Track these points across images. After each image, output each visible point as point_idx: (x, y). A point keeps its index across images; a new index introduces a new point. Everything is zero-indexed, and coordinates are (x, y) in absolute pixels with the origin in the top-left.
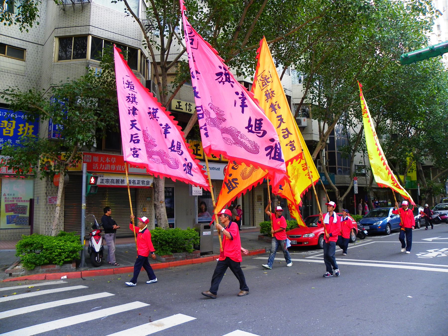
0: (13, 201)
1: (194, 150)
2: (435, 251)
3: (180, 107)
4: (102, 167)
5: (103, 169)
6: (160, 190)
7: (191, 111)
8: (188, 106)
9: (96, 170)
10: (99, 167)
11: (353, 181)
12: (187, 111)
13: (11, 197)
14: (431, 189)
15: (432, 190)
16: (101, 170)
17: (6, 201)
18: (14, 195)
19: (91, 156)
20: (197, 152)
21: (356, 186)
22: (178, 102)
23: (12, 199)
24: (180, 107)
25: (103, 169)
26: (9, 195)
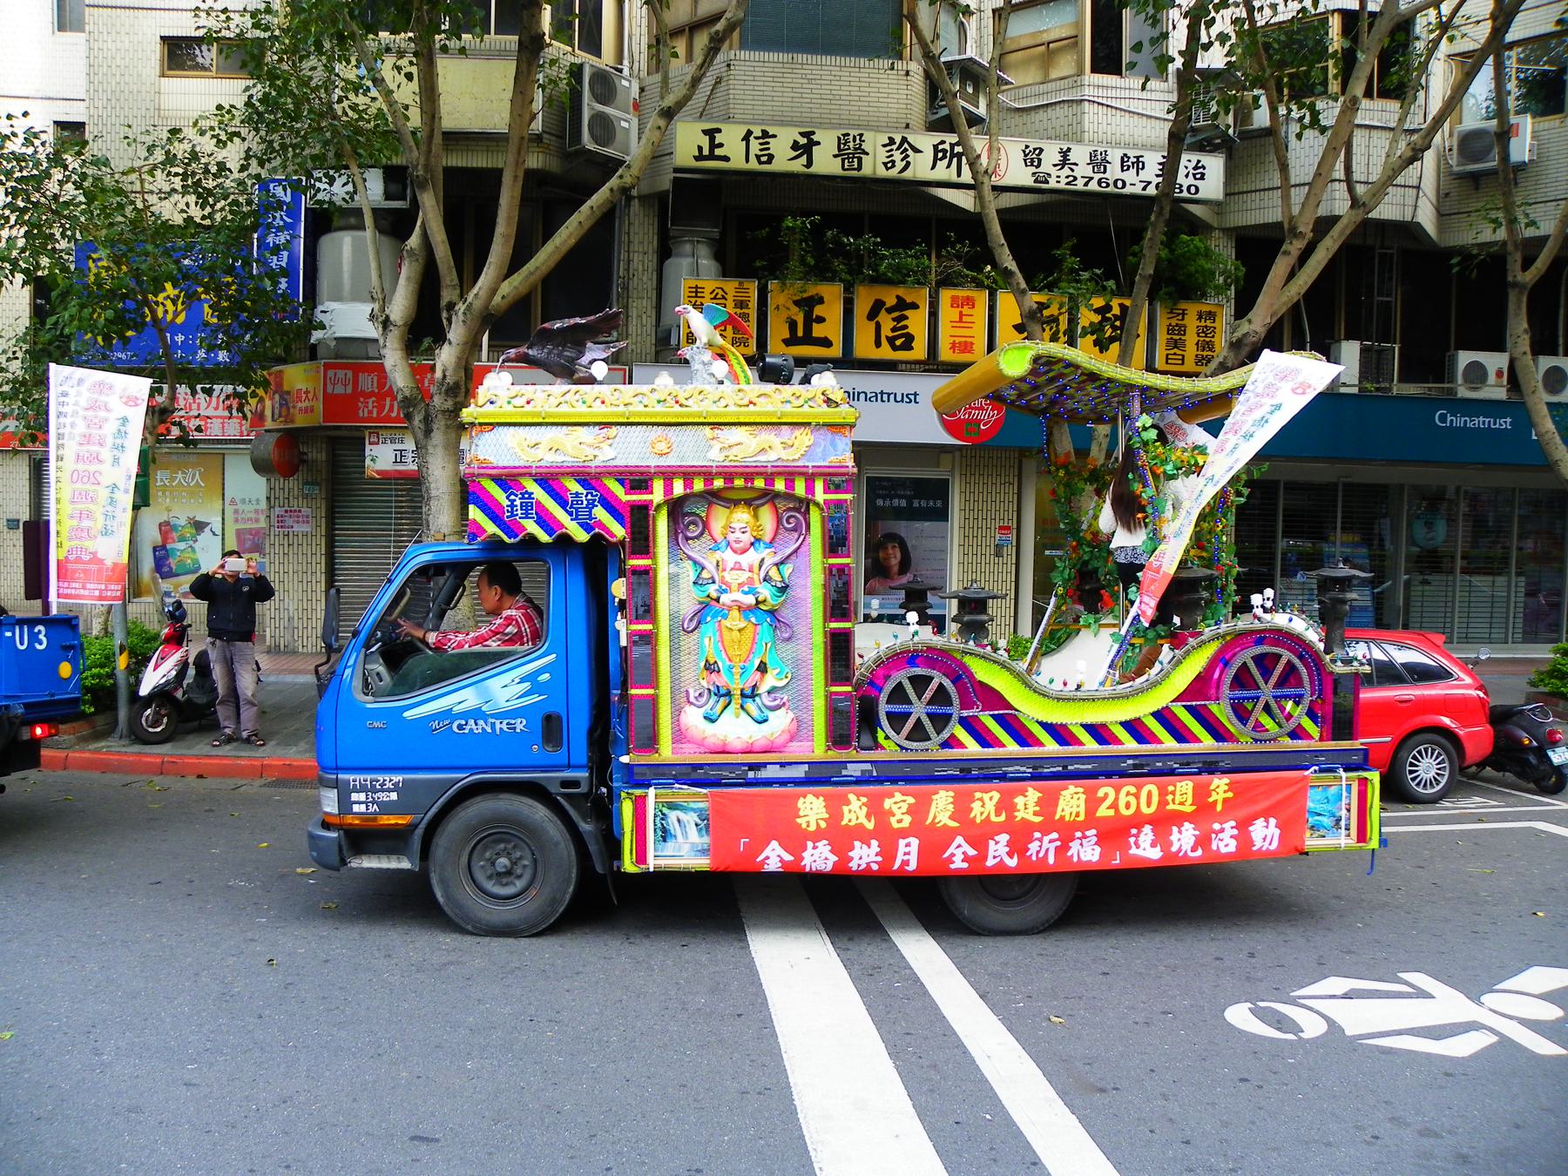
0: (257, 520)
1: (793, 325)
3: (718, 152)
4: (391, 409)
5: (394, 414)
6: (433, 493)
7: (769, 161)
8: (755, 146)
9: (370, 420)
10: (381, 409)
12: (753, 165)
13: (252, 508)
16: (388, 419)
17: (236, 521)
19: (350, 374)
22: (705, 132)
23: (253, 515)
24: (718, 152)
25: (394, 414)
26: (243, 501)
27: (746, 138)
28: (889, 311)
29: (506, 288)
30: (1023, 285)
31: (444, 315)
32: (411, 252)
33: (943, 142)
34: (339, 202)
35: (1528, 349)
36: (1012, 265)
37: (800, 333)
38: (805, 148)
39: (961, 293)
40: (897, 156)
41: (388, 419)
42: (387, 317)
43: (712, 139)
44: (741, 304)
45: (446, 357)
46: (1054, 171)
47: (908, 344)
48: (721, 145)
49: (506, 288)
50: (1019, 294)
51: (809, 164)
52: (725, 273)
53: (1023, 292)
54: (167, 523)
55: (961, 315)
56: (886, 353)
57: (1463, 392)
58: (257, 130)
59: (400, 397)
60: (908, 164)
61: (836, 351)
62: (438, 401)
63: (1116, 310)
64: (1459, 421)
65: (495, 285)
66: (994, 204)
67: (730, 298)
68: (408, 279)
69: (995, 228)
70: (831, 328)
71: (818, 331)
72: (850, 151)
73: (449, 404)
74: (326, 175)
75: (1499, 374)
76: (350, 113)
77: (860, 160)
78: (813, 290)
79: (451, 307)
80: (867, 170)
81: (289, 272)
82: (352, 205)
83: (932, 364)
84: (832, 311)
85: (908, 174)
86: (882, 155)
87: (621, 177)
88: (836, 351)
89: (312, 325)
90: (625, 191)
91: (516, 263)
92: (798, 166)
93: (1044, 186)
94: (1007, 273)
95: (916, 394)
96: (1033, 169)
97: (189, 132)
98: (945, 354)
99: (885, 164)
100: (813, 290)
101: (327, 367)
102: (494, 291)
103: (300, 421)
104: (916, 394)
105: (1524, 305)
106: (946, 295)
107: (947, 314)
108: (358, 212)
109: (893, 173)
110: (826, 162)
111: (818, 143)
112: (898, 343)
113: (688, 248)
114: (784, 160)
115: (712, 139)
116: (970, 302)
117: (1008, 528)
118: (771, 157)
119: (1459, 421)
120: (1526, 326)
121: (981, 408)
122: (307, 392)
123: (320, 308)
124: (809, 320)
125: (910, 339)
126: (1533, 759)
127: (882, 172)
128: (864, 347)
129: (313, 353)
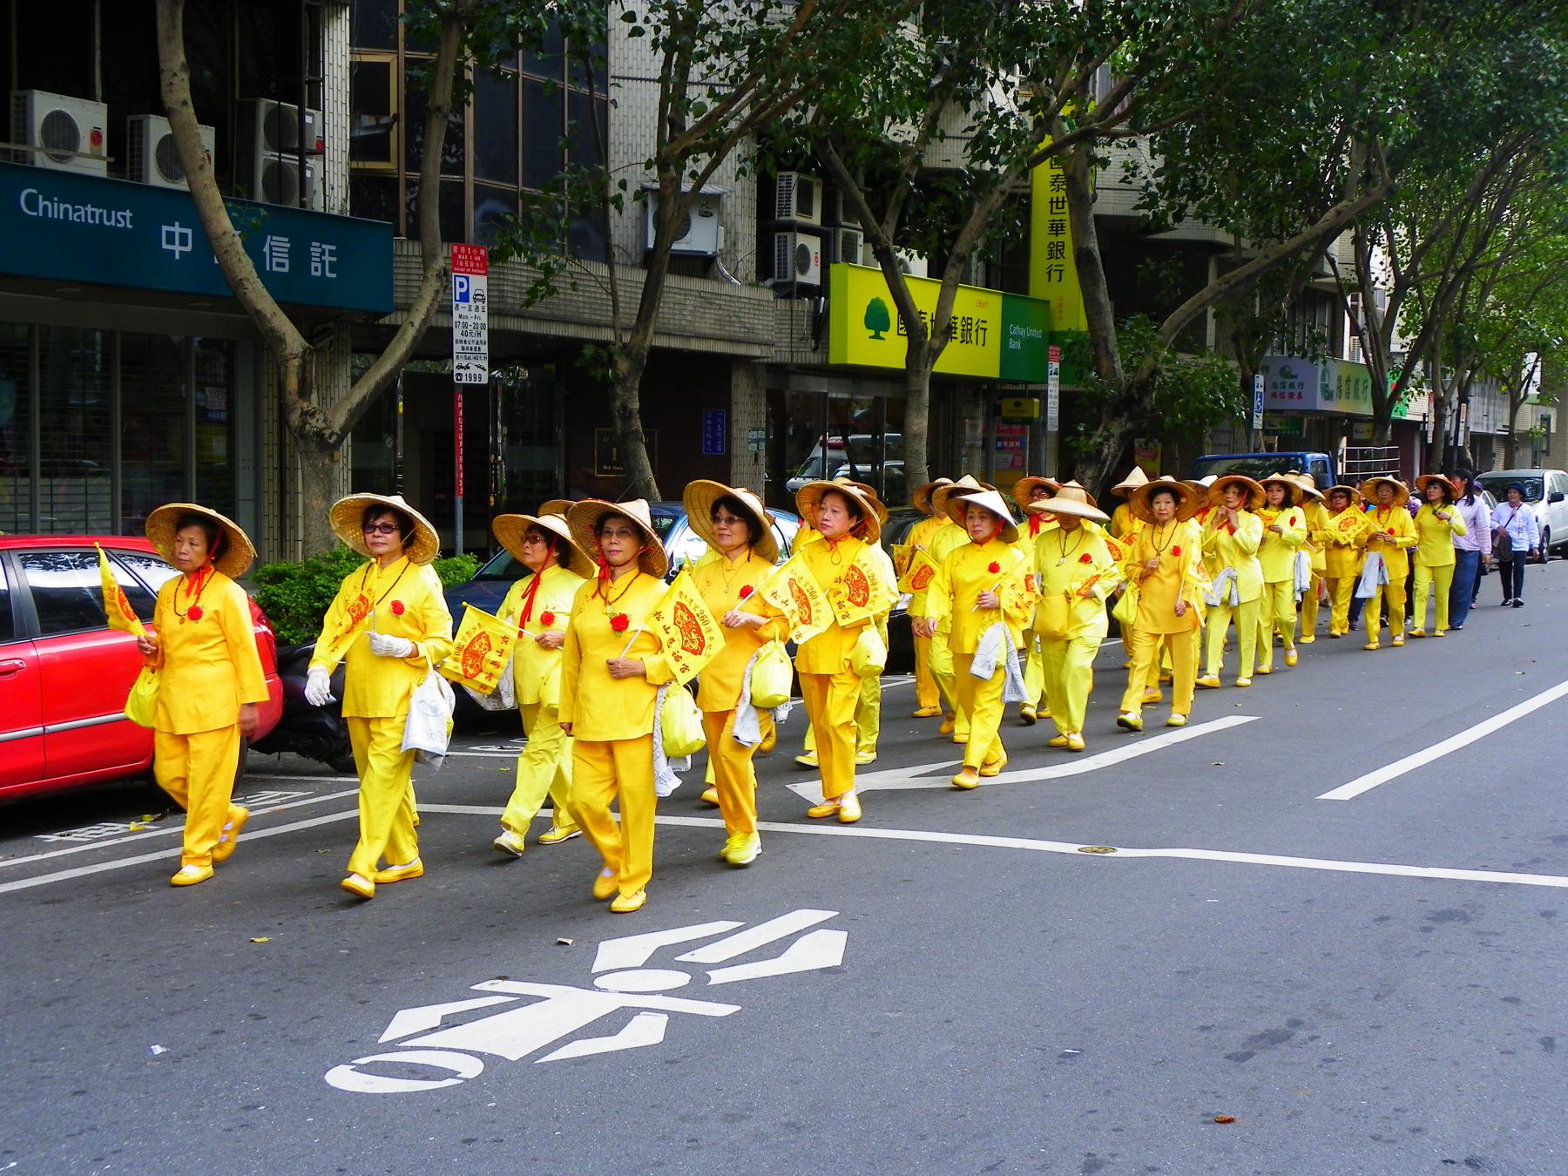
2: (662, 959)
11: (445, 275)
14: (1145, 387)
15: (1151, 400)
21: (471, 322)
35: (187, 96)
57: (42, 160)
64: (57, 210)
75: (96, 138)
105: (179, 23)
119: (57, 210)
120: (183, 59)
126: (330, 723)
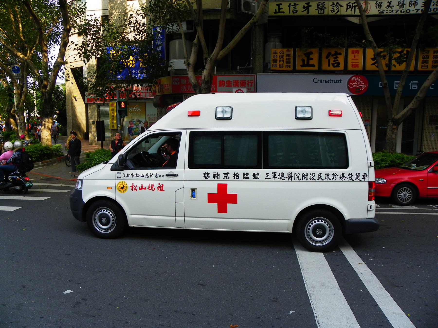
1: (303, 61)
3: (281, 10)
5: (191, 90)
7: (296, 12)
10: (187, 88)
12: (291, 14)
13: (153, 117)
18: (155, 115)
19: (179, 79)
20: (308, 62)
22: (277, 5)
24: (281, 10)
25: (191, 90)
26: (151, 115)
27: (289, 6)
28: (333, 56)
29: (221, 53)
30: (375, 45)
31: (204, 61)
32: (195, 44)
33: (350, 3)
34: (175, 32)
36: (371, 39)
37: (306, 63)
38: (307, 8)
39: (355, 49)
40: (335, 8)
41: (190, 92)
42: (189, 63)
43: (279, 7)
44: (288, 55)
45: (205, 73)
46: (385, 9)
47: (338, 66)
48: (282, 8)
49: (221, 53)
50: (374, 48)
51: (308, 12)
52: (283, 46)
53: (375, 48)
54: (131, 121)
55: (355, 56)
56: (332, 68)
58: (153, 13)
59: (193, 85)
60: (339, 10)
61: (316, 68)
62: (203, 85)
63: (405, 52)
65: (218, 52)
66: (366, 21)
67: (285, 53)
68: (194, 52)
69: (367, 28)
70: (315, 61)
71: (311, 62)
72: (321, 8)
73: (206, 86)
74: (171, 24)
76: (177, 6)
77: (324, 10)
78: (309, 50)
79: (206, 59)
80: (326, 13)
81: (162, 51)
82: (178, 32)
83: (346, 71)
84: (315, 57)
85: (339, 13)
86: (330, 8)
87: (253, 19)
88: (316, 68)
89: (168, 66)
90: (254, 23)
91: (223, 47)
92: (305, 13)
93: (383, 14)
94: (371, 42)
95: (340, 80)
96: (379, 9)
97: (135, 15)
98: (350, 68)
99: (331, 11)
100: (309, 50)
101: (173, 77)
102: (218, 54)
103: (166, 93)
104: (340, 80)
106: (350, 50)
107: (350, 56)
108: (180, 34)
109: (334, 13)
110: (313, 11)
111: (311, 6)
112: (335, 65)
113: (272, 39)
114: (301, 11)
115: (279, 7)
116: (358, 52)
117: (368, 120)
118: (297, 11)
121: (361, 84)
122: (167, 85)
123: (170, 61)
124: (309, 59)
125: (339, 63)
127: (330, 13)
128: (325, 67)
129: (168, 74)
